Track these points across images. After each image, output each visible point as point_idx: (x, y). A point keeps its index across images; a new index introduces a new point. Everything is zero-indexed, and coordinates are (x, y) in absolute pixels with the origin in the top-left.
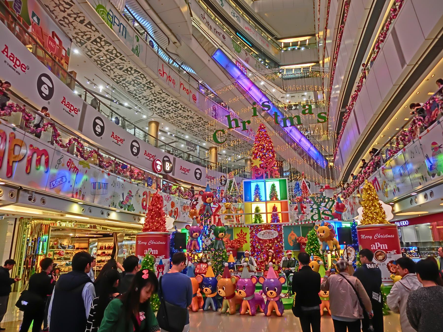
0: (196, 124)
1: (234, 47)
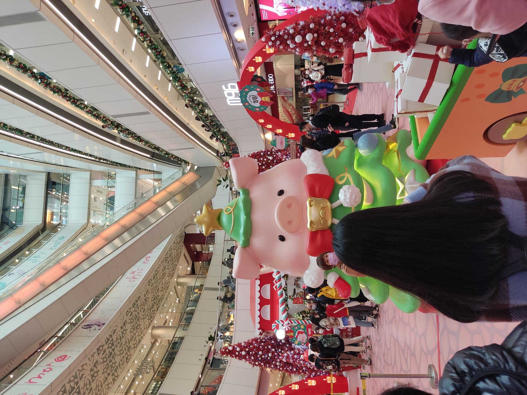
0: (109, 357)
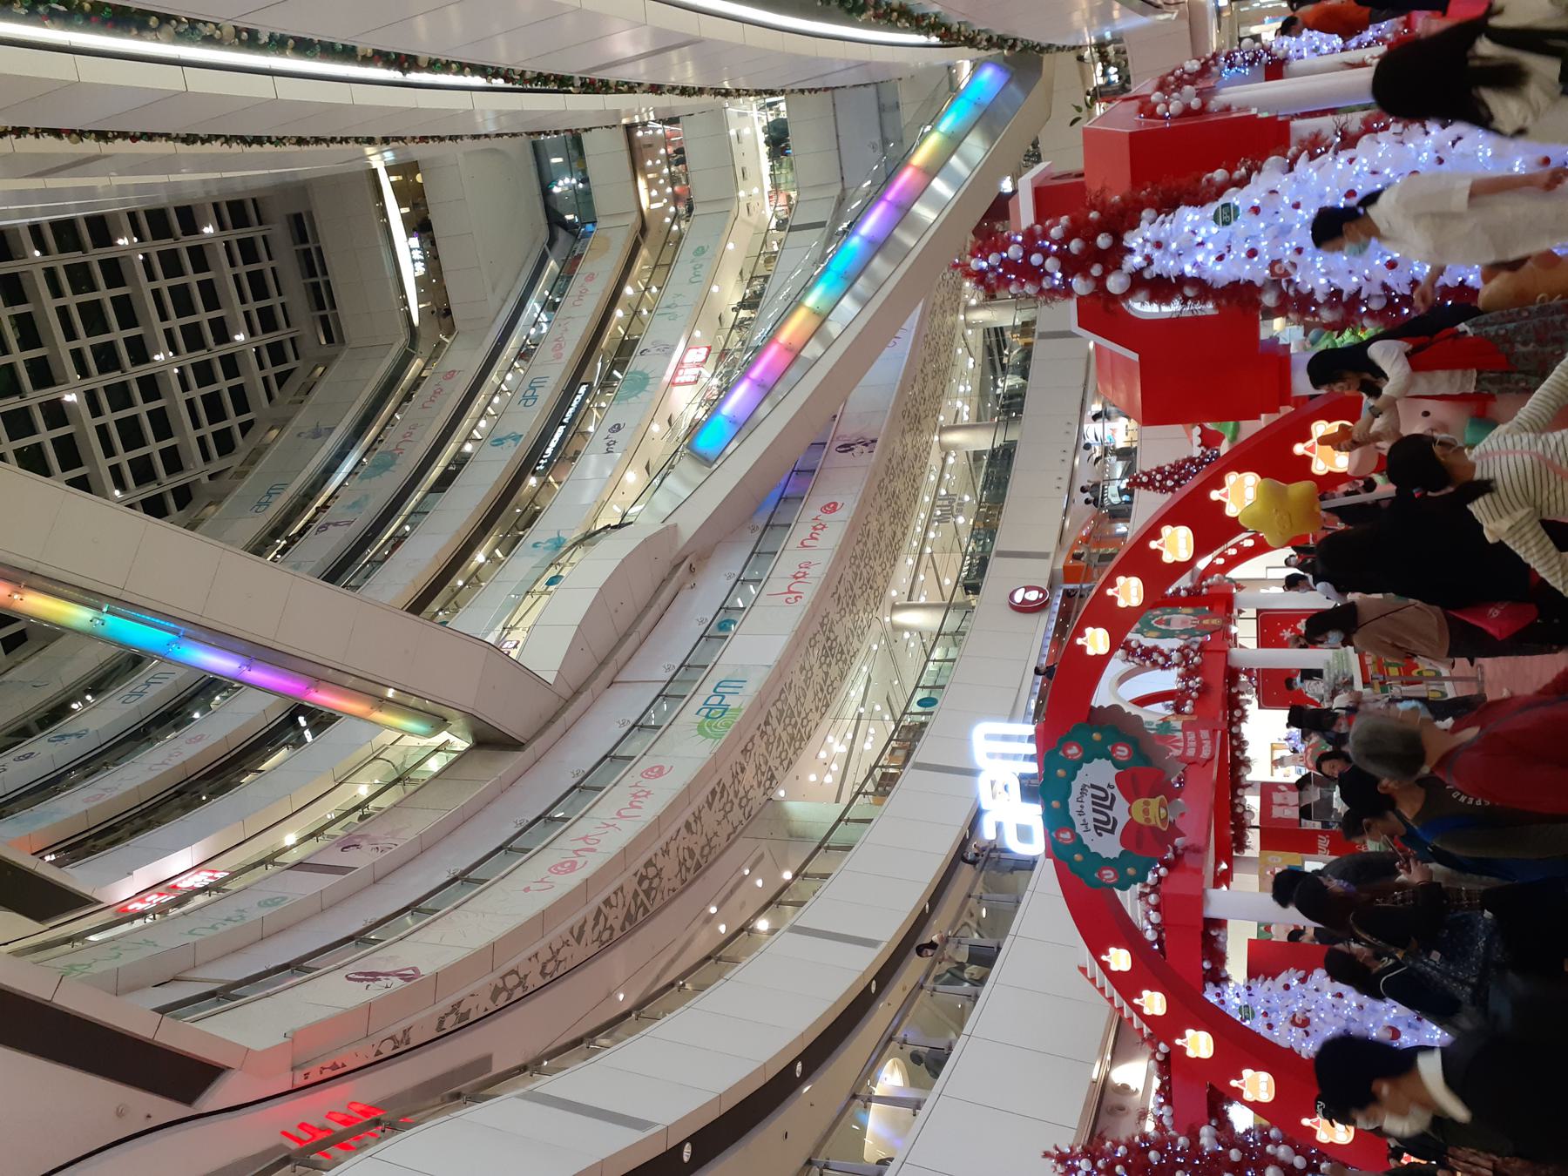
1: (636, 395)
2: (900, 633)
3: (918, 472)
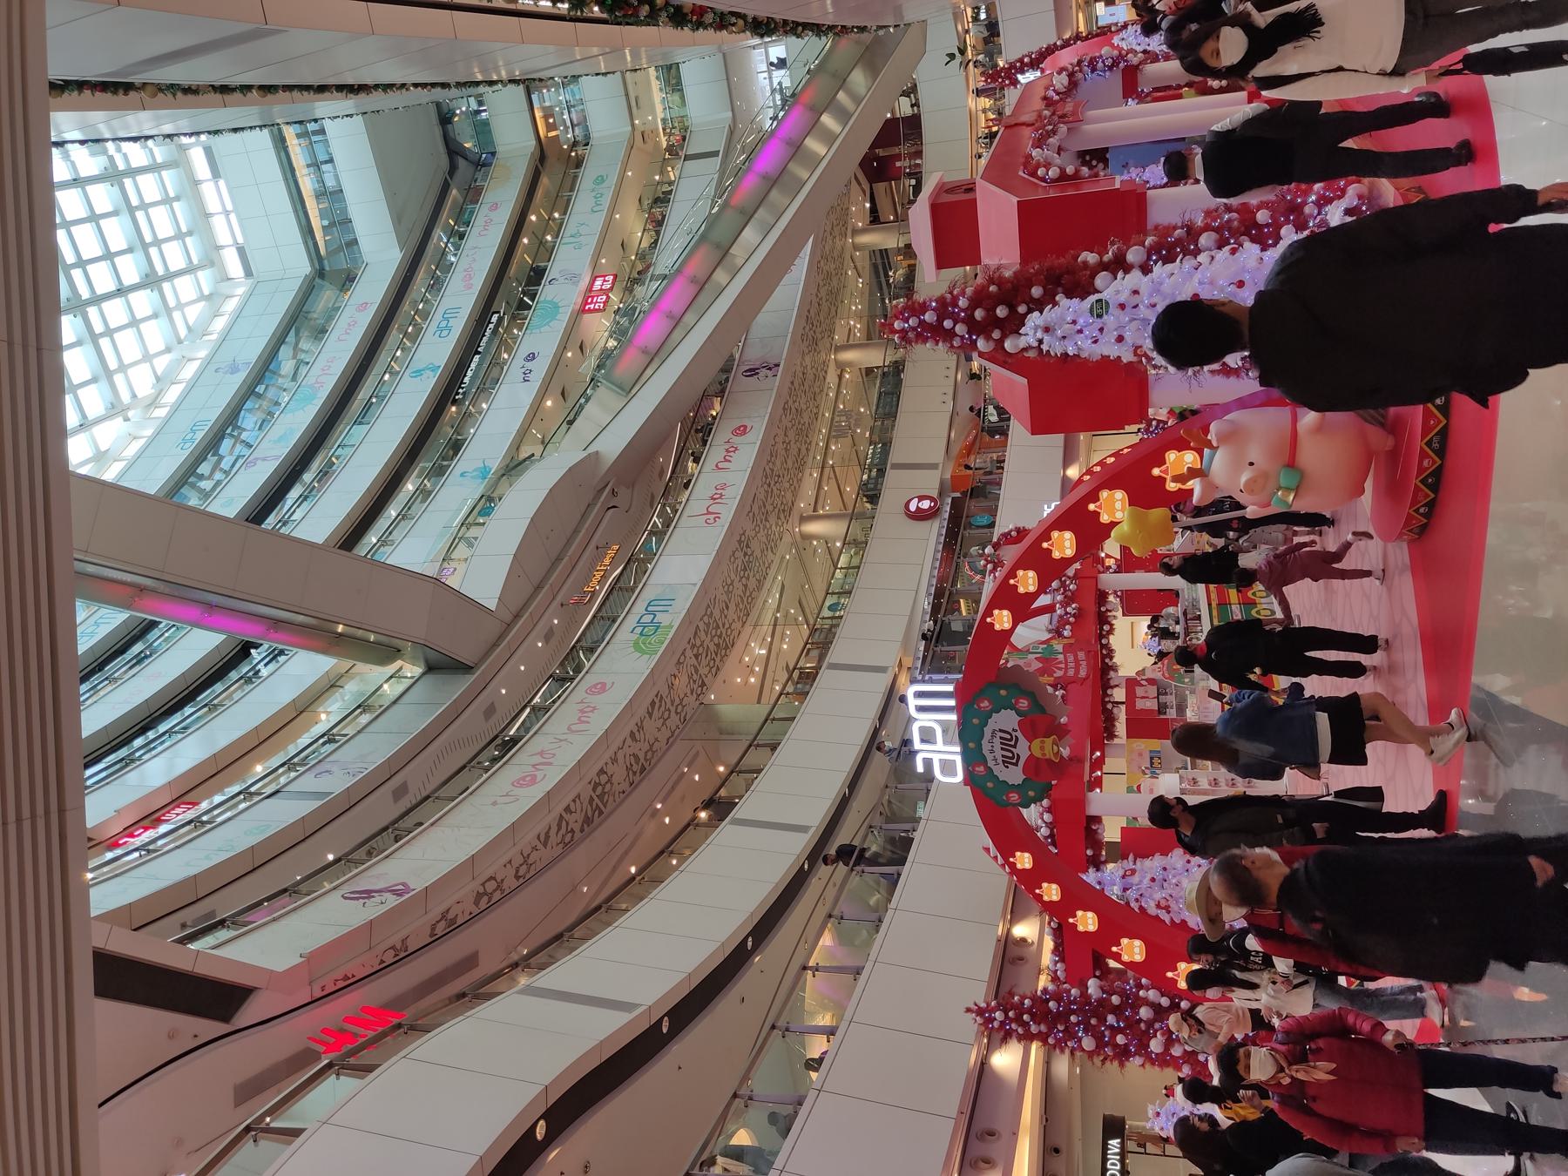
2: (808, 542)
3: (817, 390)
